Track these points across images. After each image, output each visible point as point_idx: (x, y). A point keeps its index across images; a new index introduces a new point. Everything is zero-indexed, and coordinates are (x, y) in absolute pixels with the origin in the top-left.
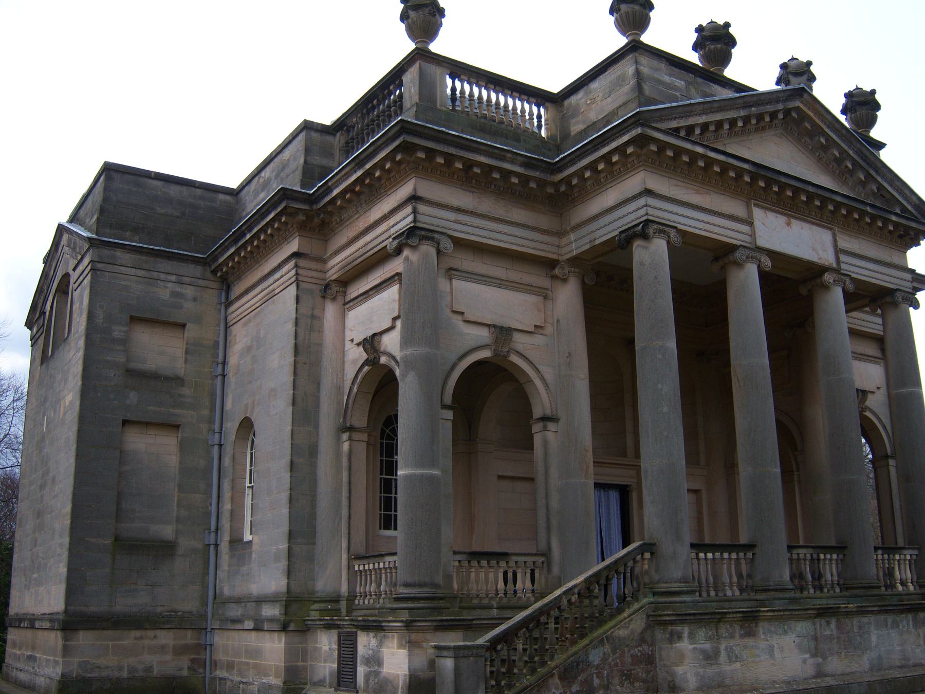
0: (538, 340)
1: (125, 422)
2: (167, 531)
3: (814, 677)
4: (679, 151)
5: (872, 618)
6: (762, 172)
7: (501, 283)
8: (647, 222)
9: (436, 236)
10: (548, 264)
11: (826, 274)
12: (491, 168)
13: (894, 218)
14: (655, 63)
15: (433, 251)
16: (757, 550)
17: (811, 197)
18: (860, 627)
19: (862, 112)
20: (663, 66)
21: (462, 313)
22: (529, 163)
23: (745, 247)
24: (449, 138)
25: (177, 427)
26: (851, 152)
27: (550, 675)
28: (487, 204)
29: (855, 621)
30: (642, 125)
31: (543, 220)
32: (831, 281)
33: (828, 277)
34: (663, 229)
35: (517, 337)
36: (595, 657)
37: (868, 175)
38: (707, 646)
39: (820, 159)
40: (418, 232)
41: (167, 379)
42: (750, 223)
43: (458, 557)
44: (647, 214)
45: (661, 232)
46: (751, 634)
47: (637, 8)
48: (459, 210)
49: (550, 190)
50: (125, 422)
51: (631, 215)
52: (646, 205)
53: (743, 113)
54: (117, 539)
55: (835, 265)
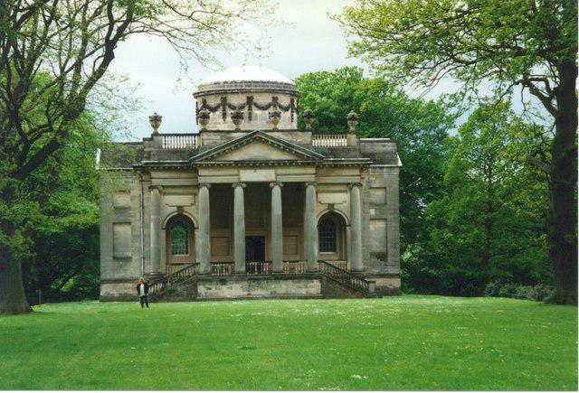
0: (193, 207)
1: (114, 224)
2: (129, 254)
7: (183, 194)
22: (181, 163)
25: (130, 223)
28: (173, 174)
31: (191, 175)
34: (204, 185)
41: (126, 208)
50: (114, 224)
54: (115, 258)
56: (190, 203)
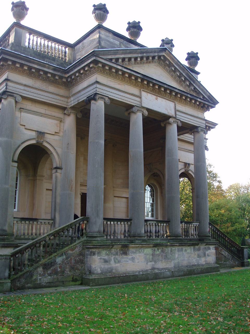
0: (56, 137)
3: (150, 270)
4: (111, 68)
5: (177, 248)
6: (145, 78)
7: (41, 115)
8: (96, 94)
9: (15, 95)
10: (64, 109)
11: (170, 119)
12: (40, 70)
13: (199, 100)
14: (107, 34)
15: (13, 101)
16: (132, 221)
17: (166, 89)
18: (171, 251)
19: (193, 60)
20: (111, 35)
21: (25, 126)
22: (55, 69)
23: (137, 106)
24: (22, 57)
26: (184, 74)
27: (38, 267)
28: (38, 84)
29: (169, 249)
30: (95, 56)
31: (62, 91)
32: (172, 121)
33: (171, 120)
34: (103, 97)
35: (47, 136)
36: (59, 260)
37: (190, 83)
38: (106, 257)
39: (172, 76)
40: (7, 93)
42: (140, 98)
43: (16, 220)
44: (96, 91)
45: (101, 98)
46: (125, 253)
47: (102, 12)
48: (25, 85)
49: (64, 80)
51: (90, 92)
52: (96, 88)
53: (140, 55)
55: (174, 116)
56: (52, 131)
